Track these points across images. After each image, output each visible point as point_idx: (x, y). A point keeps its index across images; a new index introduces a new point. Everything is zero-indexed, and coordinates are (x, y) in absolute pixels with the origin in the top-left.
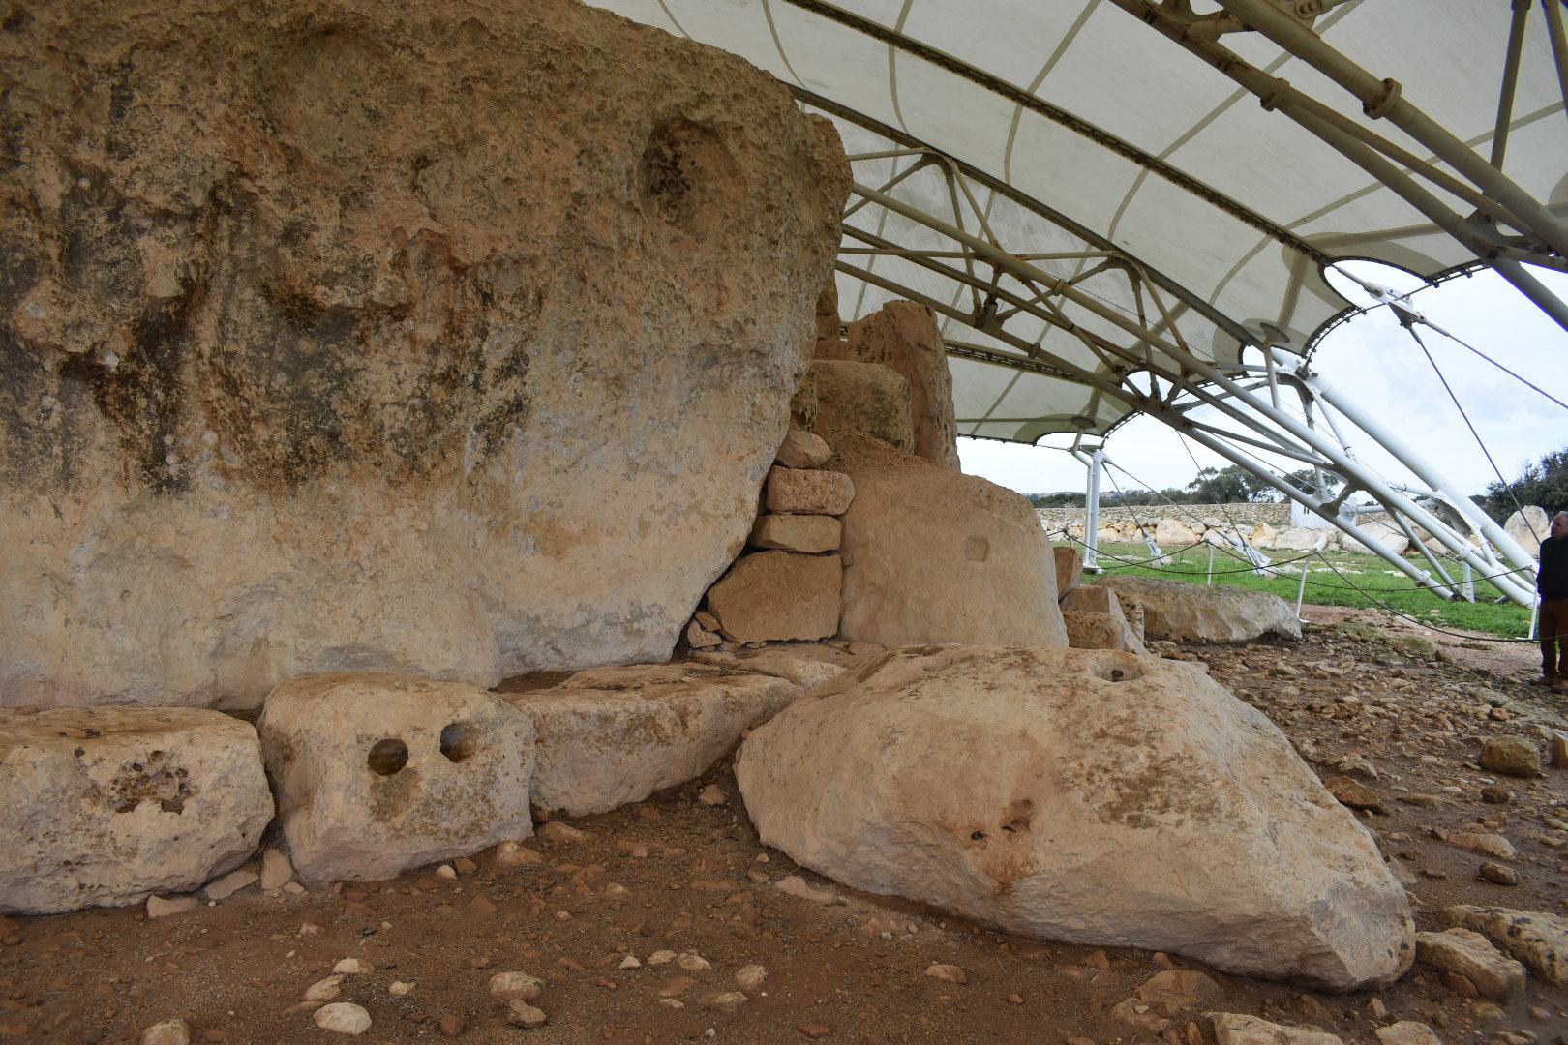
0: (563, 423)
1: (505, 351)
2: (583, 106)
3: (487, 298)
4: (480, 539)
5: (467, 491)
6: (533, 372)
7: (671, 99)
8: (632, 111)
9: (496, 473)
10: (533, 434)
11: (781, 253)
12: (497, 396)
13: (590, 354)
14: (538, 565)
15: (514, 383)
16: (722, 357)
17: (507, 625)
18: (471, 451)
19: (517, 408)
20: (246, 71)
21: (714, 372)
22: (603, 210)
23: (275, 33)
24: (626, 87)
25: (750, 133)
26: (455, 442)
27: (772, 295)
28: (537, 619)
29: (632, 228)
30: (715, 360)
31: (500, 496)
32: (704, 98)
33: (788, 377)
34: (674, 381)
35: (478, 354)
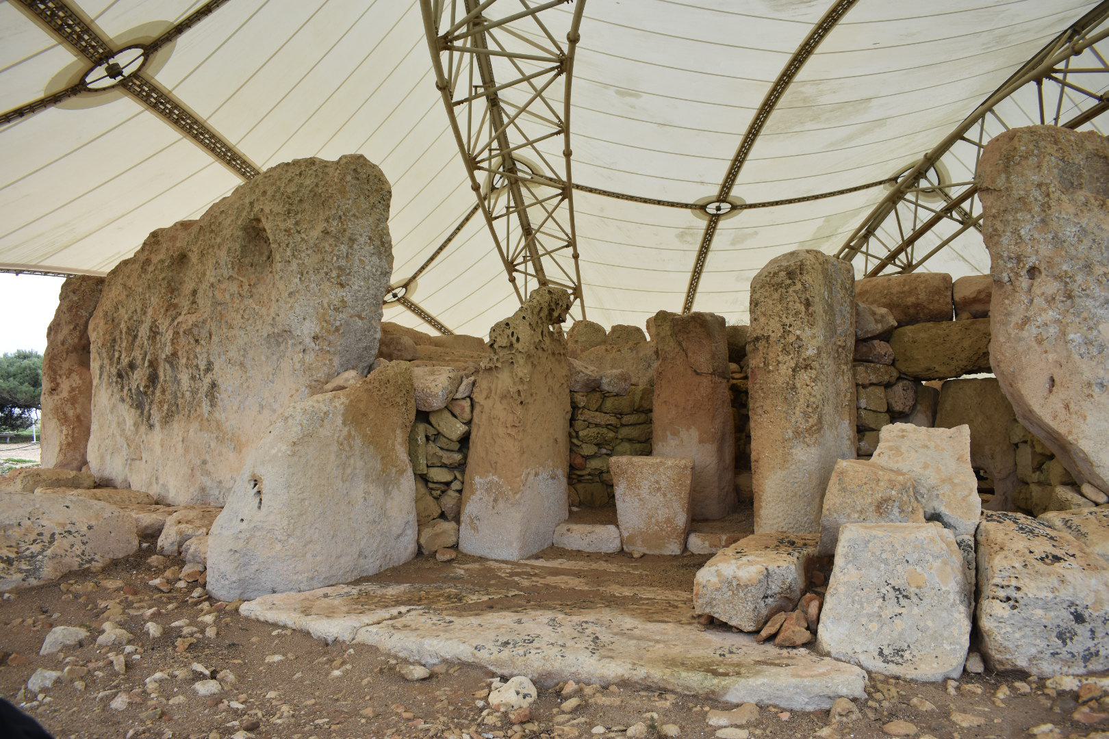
0: (230, 389)
1: (204, 362)
2: (219, 240)
3: (197, 341)
4: (213, 445)
5: (206, 423)
6: (216, 367)
7: (245, 213)
8: (227, 233)
9: (217, 415)
10: (224, 396)
11: (294, 266)
12: (207, 380)
13: (231, 354)
14: (232, 456)
15: (209, 375)
16: (280, 337)
17: (209, 483)
18: (205, 407)
19: (214, 385)
20: (164, 284)
21: (282, 347)
22: (223, 286)
23: (169, 267)
24: (229, 221)
25: (267, 210)
26: (199, 405)
27: (291, 294)
28: (220, 482)
29: (234, 287)
30: (279, 344)
31: (219, 427)
32: (251, 204)
33: (308, 340)
34: (263, 358)
35: (197, 366)
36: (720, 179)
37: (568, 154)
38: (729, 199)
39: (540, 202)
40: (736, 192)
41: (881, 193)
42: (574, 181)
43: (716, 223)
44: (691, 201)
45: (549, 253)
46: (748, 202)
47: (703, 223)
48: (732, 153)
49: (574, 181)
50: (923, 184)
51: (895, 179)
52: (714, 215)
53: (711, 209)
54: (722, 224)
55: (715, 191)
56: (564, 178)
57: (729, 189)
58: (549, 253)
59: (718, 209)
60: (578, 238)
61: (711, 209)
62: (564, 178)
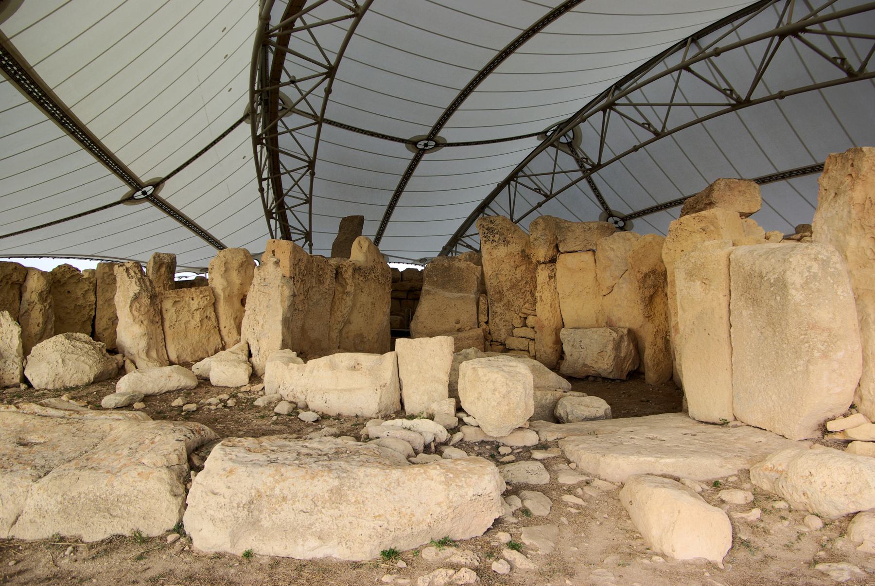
36: (433, 122)
37: (328, 91)
38: (436, 139)
39: (290, 131)
40: (443, 133)
41: (535, 142)
42: (325, 117)
43: (421, 156)
44: (407, 138)
45: (288, 172)
46: (448, 142)
47: (412, 155)
48: (447, 104)
49: (325, 117)
50: (563, 140)
51: (545, 132)
52: (421, 149)
53: (421, 145)
54: (426, 156)
55: (427, 131)
56: (319, 114)
57: (439, 130)
58: (288, 172)
59: (426, 145)
60: (317, 162)
61: (421, 145)
62: (319, 114)
